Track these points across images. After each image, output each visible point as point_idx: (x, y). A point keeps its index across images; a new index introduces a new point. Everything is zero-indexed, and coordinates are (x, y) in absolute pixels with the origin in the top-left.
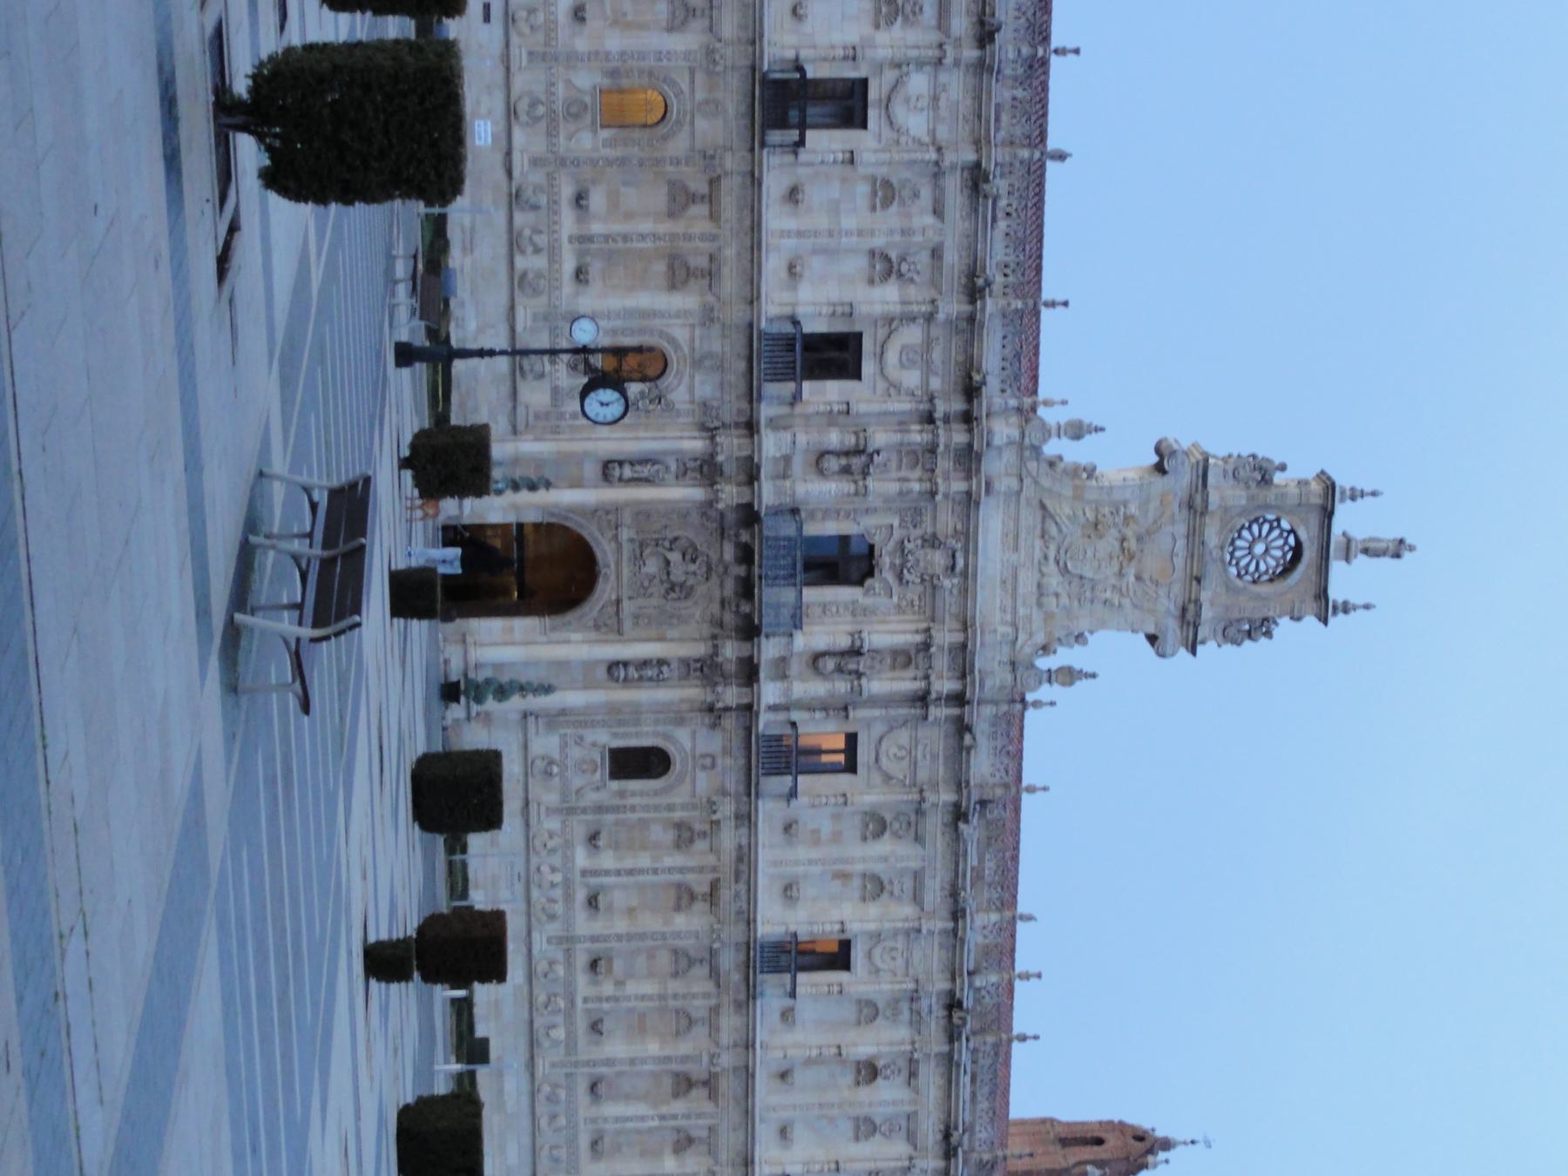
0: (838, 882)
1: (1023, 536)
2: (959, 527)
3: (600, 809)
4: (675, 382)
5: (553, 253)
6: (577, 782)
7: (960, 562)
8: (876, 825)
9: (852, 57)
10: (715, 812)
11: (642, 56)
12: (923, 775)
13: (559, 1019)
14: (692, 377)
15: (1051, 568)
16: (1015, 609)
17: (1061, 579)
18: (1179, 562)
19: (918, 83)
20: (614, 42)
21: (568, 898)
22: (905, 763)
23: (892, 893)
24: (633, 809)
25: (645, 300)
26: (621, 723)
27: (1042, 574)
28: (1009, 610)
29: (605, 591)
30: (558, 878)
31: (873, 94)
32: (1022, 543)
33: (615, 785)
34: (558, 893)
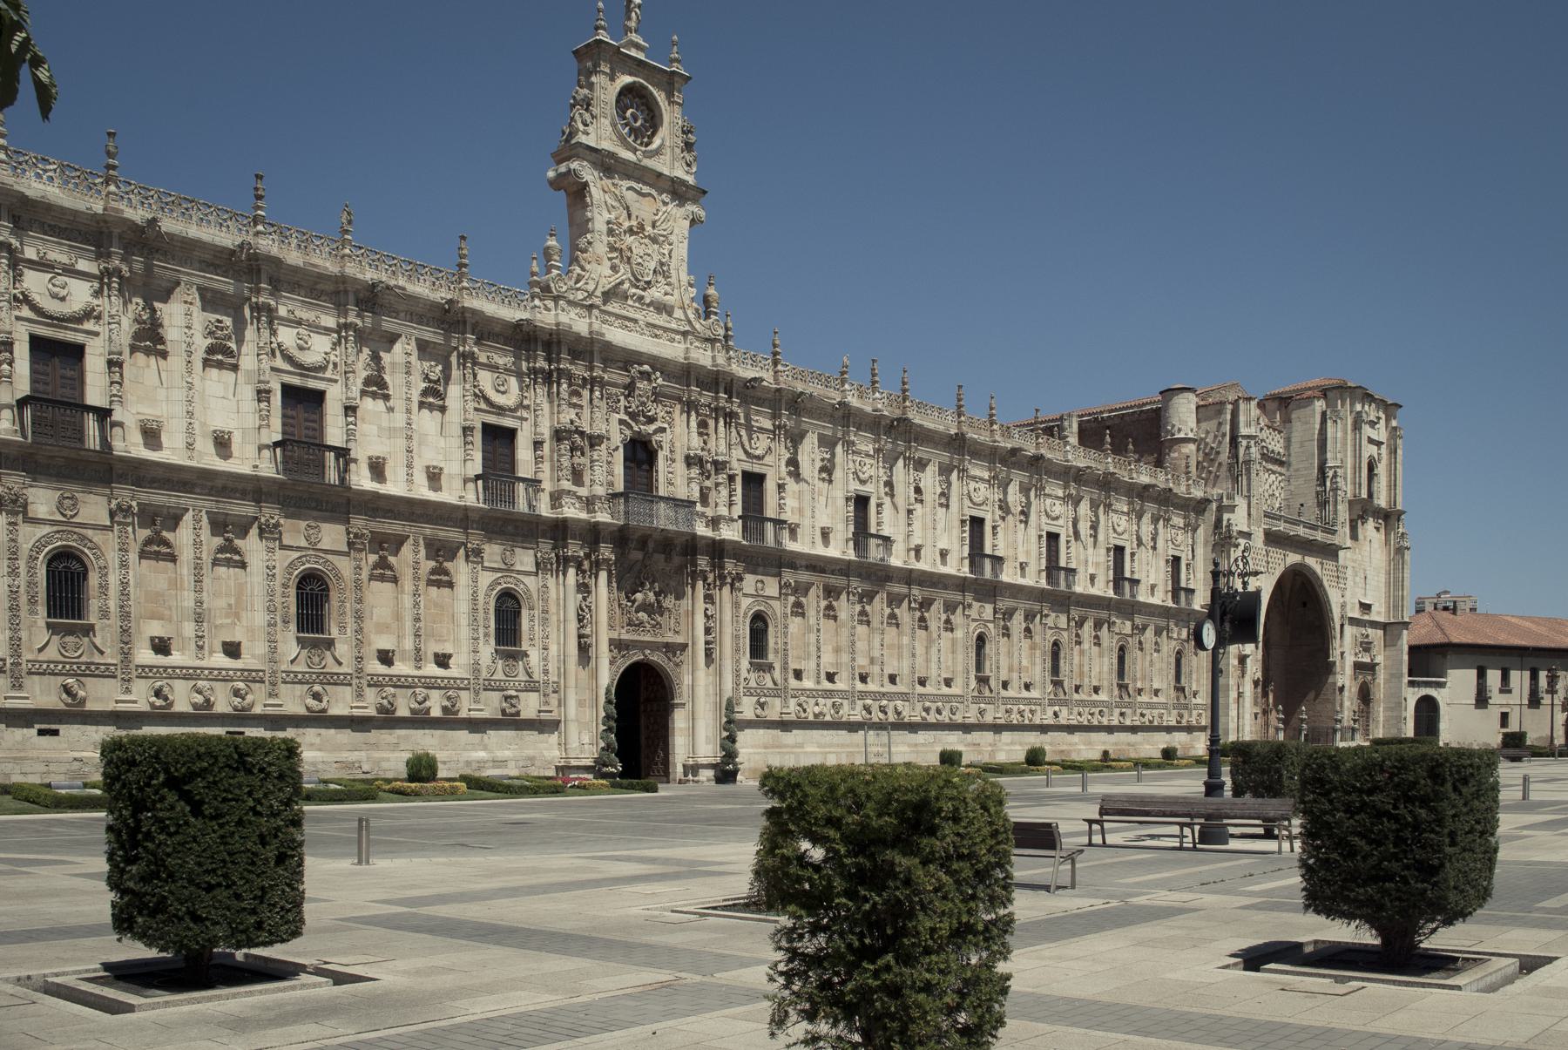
1: (624, 313)
2: (620, 364)
3: (785, 668)
4: (522, 586)
7: (646, 368)
9: (262, 395)
10: (790, 584)
11: (271, 594)
12: (768, 424)
14: (519, 572)
16: (673, 331)
17: (654, 288)
20: (260, 618)
22: (760, 436)
25: (462, 607)
27: (648, 305)
28: (673, 335)
29: (656, 658)
32: (631, 315)
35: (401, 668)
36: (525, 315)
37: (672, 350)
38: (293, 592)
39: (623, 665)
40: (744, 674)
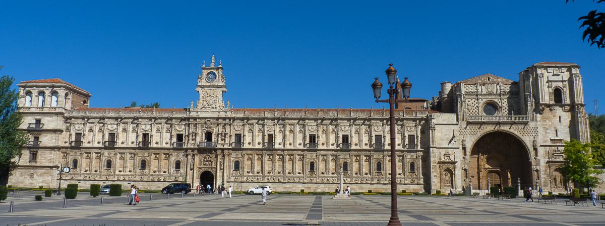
5: (161, 176)
18: (212, 88)
19: (143, 127)
21: (257, 176)
26: (230, 168)
31: (144, 133)
35: (157, 173)
37: (216, 115)
38: (140, 163)
40: (231, 172)
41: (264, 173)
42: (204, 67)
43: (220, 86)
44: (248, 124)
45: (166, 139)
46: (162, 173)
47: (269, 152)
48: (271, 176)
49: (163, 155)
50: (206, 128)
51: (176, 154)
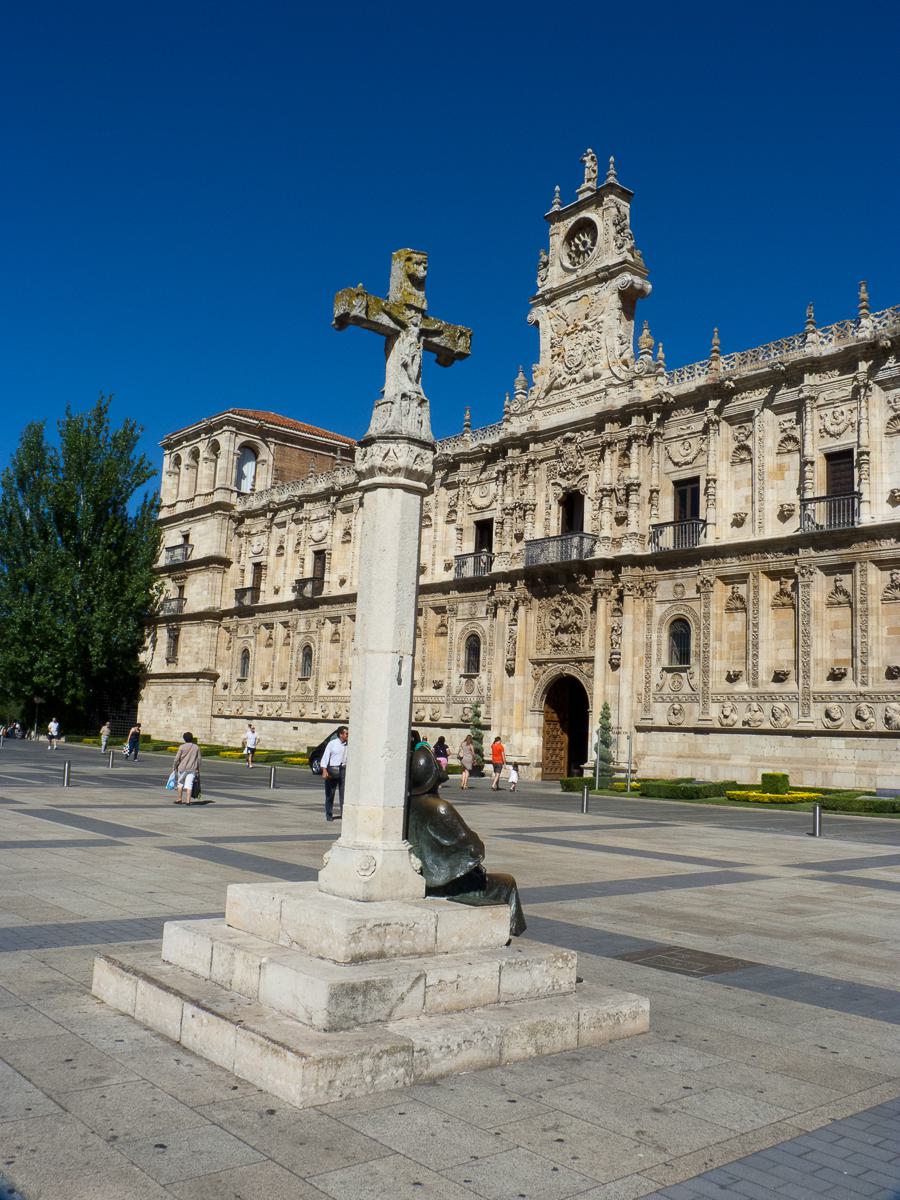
0: (787, 473)
6: (686, 689)
7: (568, 435)
8: (743, 452)
13: (879, 709)
14: (478, 619)
15: (577, 377)
18: (579, 294)
21: (772, 697)
23: (793, 428)
24: (707, 645)
26: (648, 657)
28: (598, 396)
29: (571, 670)
30: (755, 706)
33: (692, 660)
34: (767, 707)
36: (502, 435)
37: (592, 409)
39: (545, 679)
40: (655, 679)
41: (807, 676)
42: (556, 208)
43: (607, 268)
44: (731, 420)
45: (445, 550)
46: (430, 691)
47: (830, 556)
48: (846, 698)
49: (432, 613)
50: (563, 476)
51: (467, 605)
